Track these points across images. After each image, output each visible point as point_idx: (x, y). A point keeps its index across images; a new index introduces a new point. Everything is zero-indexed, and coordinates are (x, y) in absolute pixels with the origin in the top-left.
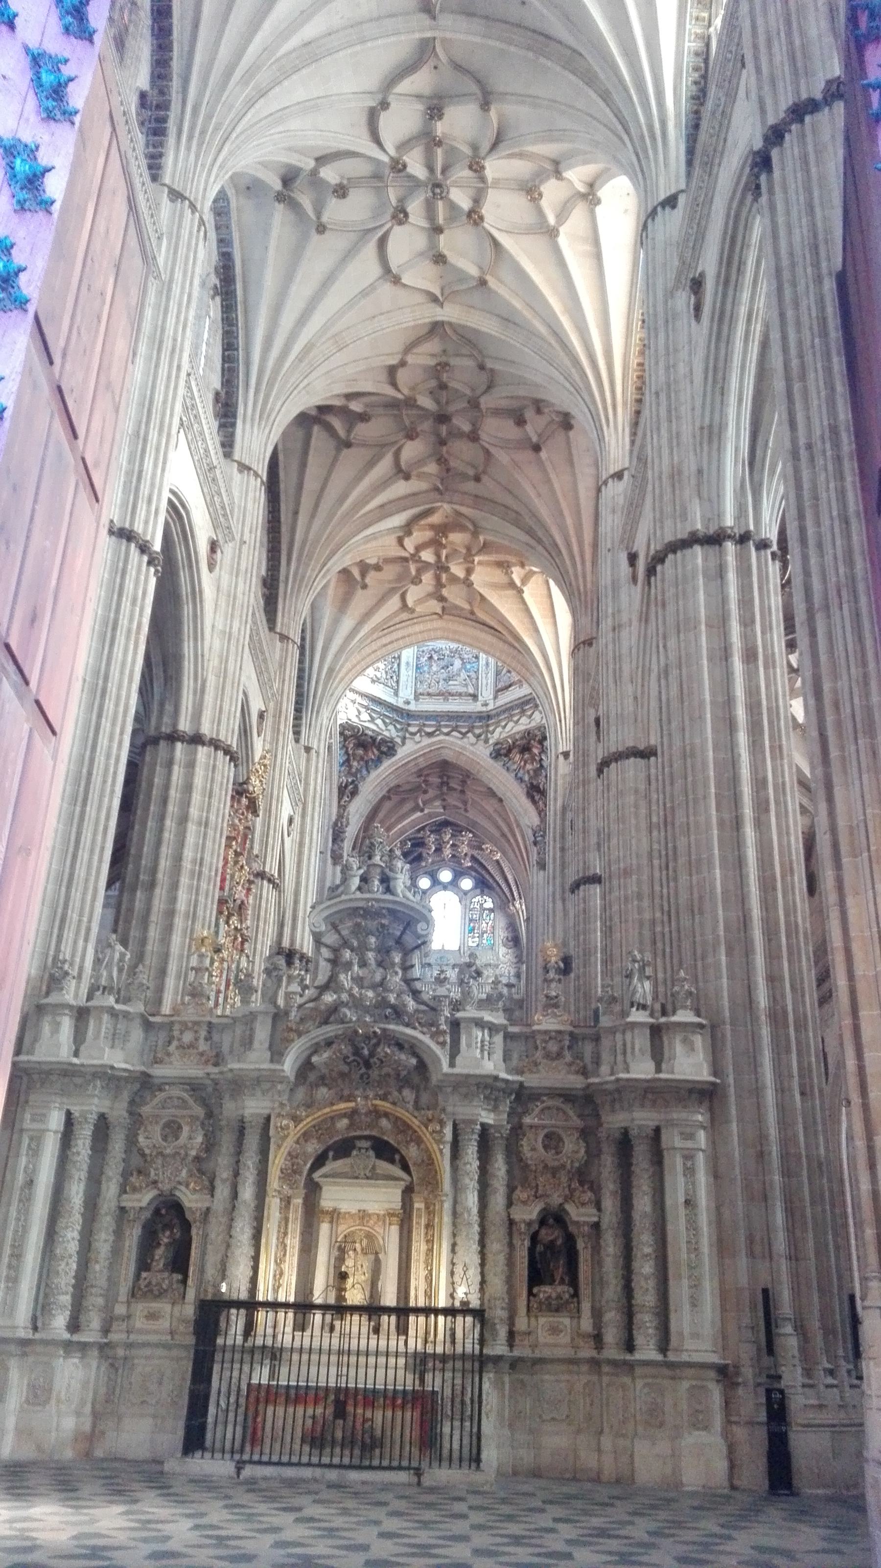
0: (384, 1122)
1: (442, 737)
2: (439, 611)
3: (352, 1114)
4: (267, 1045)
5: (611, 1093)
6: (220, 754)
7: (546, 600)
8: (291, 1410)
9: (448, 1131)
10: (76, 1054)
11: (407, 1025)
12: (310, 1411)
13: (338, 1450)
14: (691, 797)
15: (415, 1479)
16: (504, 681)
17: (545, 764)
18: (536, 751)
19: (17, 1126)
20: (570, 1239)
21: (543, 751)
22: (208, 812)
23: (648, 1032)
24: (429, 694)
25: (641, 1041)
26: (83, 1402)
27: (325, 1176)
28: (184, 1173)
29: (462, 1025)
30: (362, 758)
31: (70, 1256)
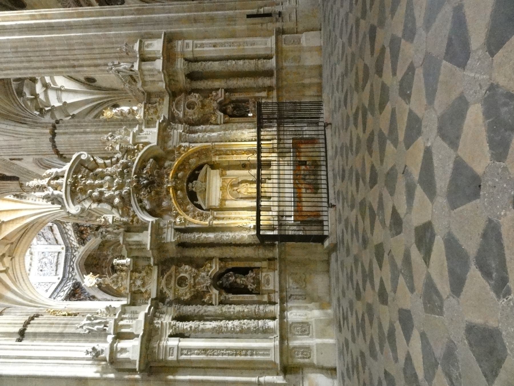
0: (179, 175)
1: (75, 265)
2: (10, 258)
3: (175, 189)
4: (141, 234)
5: (170, 80)
6: (32, 322)
7: (9, 213)
8: (304, 199)
9: (184, 144)
10: (138, 336)
11: (134, 163)
12: (304, 195)
13: (319, 177)
14: (37, 49)
15: (329, 126)
16: (53, 241)
17: (88, 225)
18: (83, 228)
19: (177, 365)
20: (232, 102)
21: (83, 226)
22: (59, 324)
23: (143, 63)
24: (56, 270)
25: (147, 66)
26: (306, 308)
27: (205, 204)
28: (203, 274)
29: (136, 141)
30: (80, 295)
31: (241, 323)
